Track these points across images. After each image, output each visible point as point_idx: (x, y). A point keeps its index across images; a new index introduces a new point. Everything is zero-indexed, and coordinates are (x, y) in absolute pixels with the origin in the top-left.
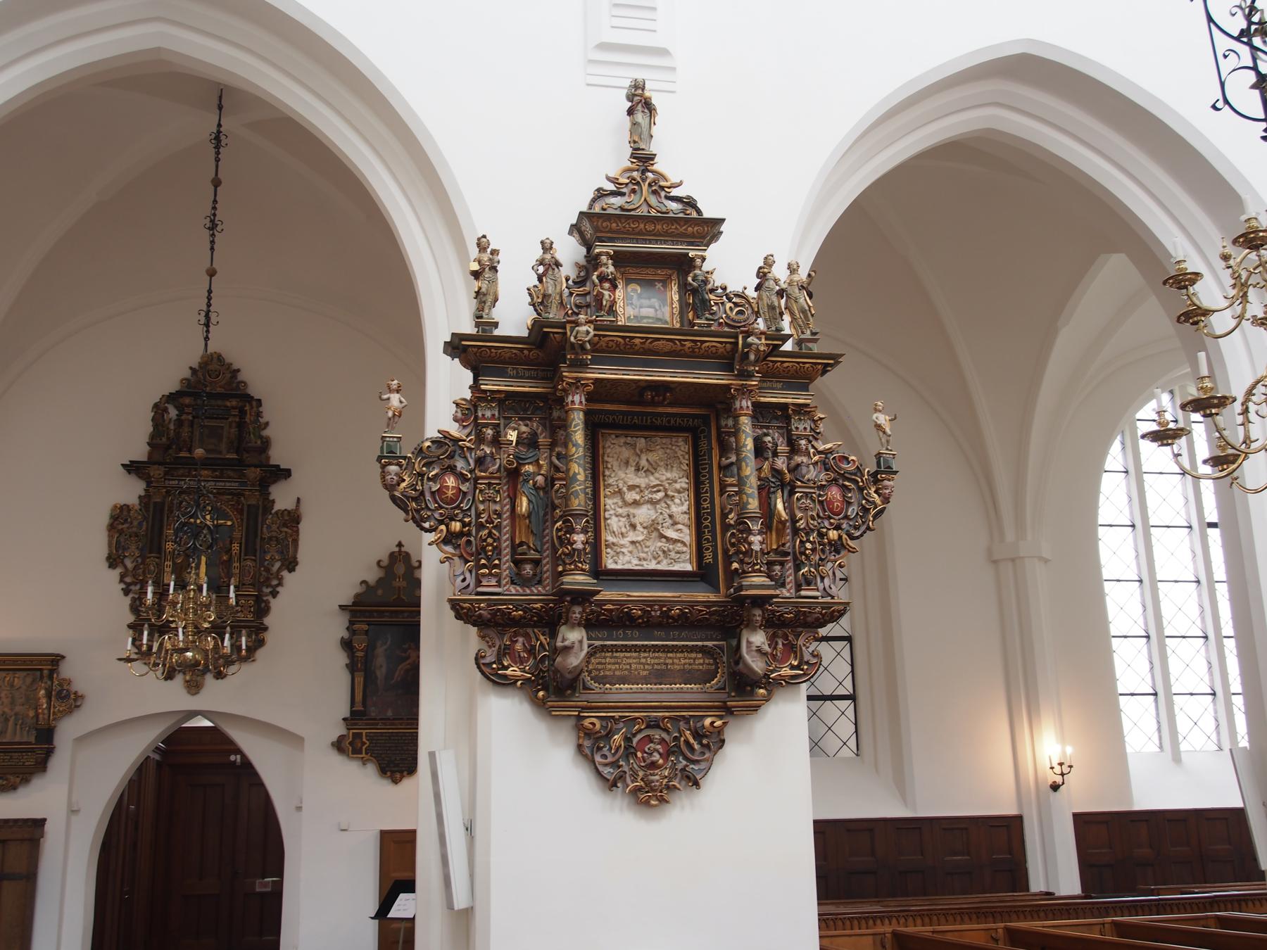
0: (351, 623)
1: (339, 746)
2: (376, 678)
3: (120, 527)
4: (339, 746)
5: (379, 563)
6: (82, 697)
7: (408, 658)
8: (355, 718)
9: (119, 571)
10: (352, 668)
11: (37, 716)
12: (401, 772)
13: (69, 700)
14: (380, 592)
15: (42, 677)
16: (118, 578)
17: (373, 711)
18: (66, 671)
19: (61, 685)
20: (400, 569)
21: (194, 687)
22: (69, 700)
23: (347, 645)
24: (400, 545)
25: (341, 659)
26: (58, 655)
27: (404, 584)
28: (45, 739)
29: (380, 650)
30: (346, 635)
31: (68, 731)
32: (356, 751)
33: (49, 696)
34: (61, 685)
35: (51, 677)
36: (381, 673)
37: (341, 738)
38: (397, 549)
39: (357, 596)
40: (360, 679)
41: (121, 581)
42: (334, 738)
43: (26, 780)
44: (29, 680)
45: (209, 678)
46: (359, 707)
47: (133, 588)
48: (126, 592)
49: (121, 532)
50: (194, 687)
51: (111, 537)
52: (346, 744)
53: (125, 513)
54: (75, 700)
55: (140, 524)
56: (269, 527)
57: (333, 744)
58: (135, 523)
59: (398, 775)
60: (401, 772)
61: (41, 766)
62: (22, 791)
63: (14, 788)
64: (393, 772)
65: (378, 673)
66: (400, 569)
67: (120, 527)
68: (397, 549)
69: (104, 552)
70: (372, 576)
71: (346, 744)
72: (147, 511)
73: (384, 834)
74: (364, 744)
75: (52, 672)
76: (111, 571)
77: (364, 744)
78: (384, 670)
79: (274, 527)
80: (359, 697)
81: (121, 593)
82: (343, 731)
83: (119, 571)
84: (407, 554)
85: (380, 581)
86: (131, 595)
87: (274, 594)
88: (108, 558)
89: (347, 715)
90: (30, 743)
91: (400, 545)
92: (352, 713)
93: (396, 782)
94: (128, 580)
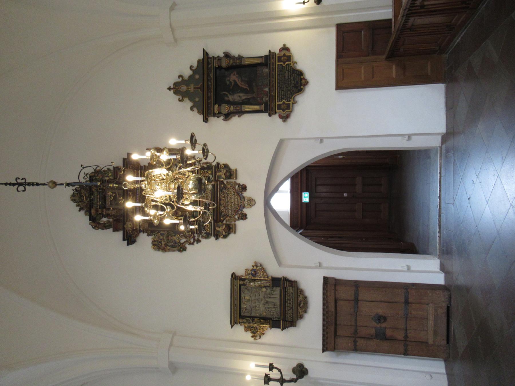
0: (214, 115)
1: (285, 118)
2: (246, 99)
3: (163, 245)
4: (285, 118)
5: (180, 101)
6: (255, 263)
8: (269, 110)
9: (187, 246)
10: (241, 113)
11: (265, 287)
12: (301, 79)
13: (257, 270)
14: (197, 99)
15: (244, 285)
16: (191, 246)
17: (265, 99)
18: (241, 272)
19: (248, 274)
20: (184, 88)
21: (251, 202)
23: (227, 117)
24: (169, 89)
25: (235, 120)
26: (232, 277)
27: (192, 86)
28: (276, 282)
29: (231, 98)
30: (222, 118)
31: (274, 270)
33: (254, 281)
34: (248, 274)
35: (244, 280)
36: (243, 96)
37: (281, 117)
38: (172, 90)
39: (199, 112)
40: (247, 108)
41: (193, 244)
42: (280, 121)
43: (301, 292)
44: (246, 292)
45: (245, 194)
46: (262, 107)
47: (196, 238)
48: (199, 241)
49: (166, 245)
51: (169, 250)
52: (284, 114)
53: (156, 243)
54: (257, 266)
55: (162, 235)
57: (284, 121)
58: (161, 237)
59: (303, 81)
60: (301, 79)
61: (293, 284)
62: (308, 293)
63: (305, 298)
64: (301, 85)
65: (244, 98)
66: (184, 88)
67: (163, 245)
68: (172, 90)
69: (177, 254)
70: (188, 104)
71: (284, 114)
72: (155, 231)
73: (339, 87)
74: (284, 103)
75: (241, 279)
76: (187, 250)
77: (284, 103)
78: (241, 95)
80: (256, 108)
81: (199, 244)
82: (277, 115)
83: (187, 246)
84: (175, 84)
85: (190, 100)
86: (200, 239)
88: (180, 251)
89: (267, 114)
91: (169, 89)
92: (265, 111)
93: (307, 83)
94: (192, 240)
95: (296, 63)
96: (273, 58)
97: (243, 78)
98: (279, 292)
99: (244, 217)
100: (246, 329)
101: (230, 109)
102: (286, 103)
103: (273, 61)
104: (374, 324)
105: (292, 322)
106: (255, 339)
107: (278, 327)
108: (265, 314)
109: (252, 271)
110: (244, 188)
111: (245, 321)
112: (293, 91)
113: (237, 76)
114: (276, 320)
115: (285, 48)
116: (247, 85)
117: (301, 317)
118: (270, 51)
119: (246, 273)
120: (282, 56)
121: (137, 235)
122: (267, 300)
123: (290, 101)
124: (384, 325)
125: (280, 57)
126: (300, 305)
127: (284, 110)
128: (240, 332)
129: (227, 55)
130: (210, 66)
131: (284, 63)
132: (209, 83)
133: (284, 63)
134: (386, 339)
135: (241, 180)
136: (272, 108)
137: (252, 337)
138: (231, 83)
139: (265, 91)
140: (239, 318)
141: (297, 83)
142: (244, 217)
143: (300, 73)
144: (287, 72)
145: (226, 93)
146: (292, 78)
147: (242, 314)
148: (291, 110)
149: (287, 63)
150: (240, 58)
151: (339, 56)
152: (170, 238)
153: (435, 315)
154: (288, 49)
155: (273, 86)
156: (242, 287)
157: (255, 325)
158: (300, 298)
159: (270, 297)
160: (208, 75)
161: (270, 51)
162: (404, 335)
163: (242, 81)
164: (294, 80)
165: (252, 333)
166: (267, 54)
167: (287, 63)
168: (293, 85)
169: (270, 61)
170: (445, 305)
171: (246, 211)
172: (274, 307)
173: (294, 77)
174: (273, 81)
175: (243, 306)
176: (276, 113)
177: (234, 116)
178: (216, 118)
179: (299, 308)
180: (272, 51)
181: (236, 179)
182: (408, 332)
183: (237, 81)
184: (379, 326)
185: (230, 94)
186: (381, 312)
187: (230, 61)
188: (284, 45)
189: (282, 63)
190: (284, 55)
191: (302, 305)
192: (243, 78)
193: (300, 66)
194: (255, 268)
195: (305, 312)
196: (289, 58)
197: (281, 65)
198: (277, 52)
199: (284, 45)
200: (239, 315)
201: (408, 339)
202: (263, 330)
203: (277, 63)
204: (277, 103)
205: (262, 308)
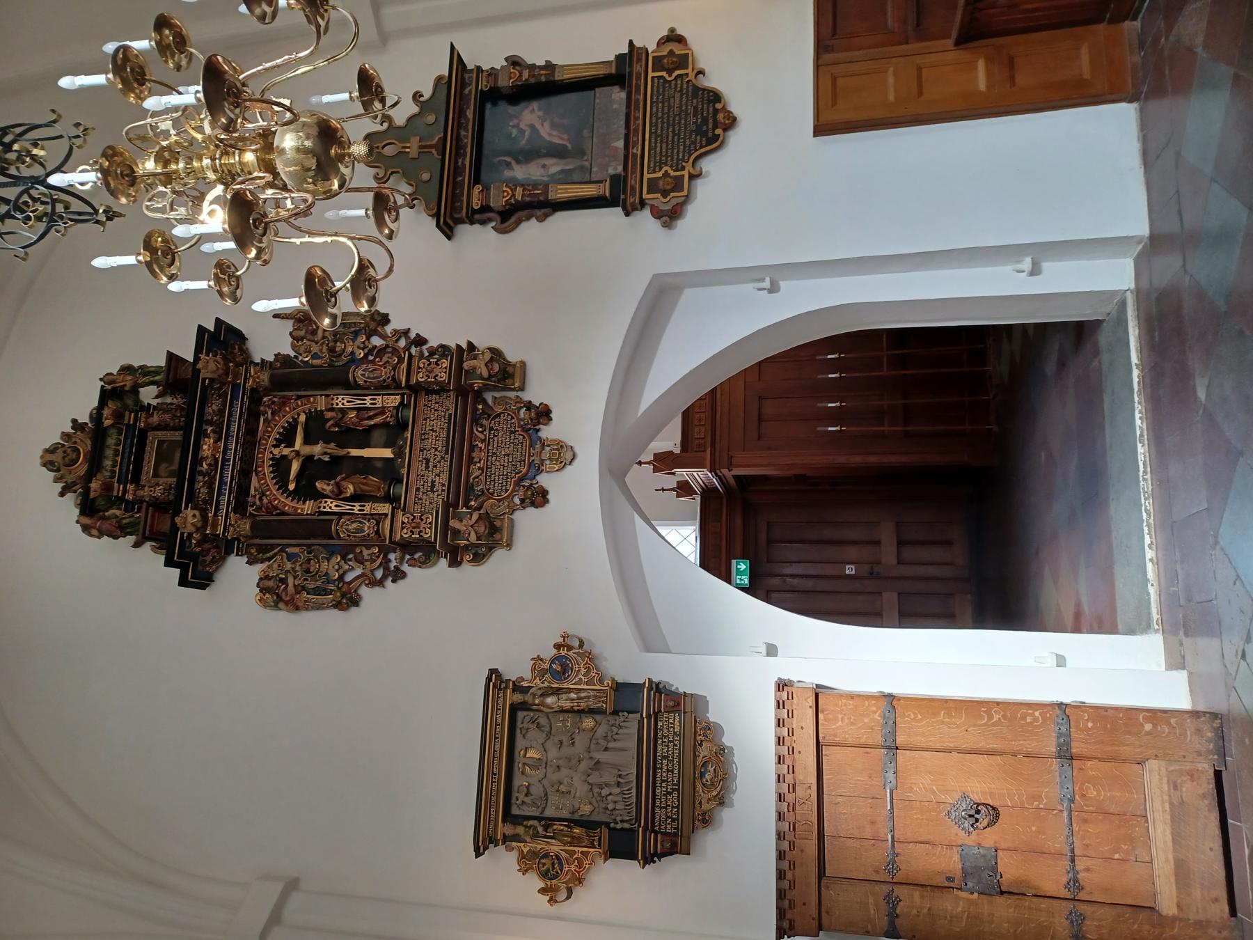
2: (562, 171)
3: (291, 588)
4: (670, 217)
7: (532, 127)
9: (364, 591)
12: (716, 111)
13: (568, 658)
15: (524, 706)
16: (377, 590)
18: (517, 668)
21: (563, 455)
22: (568, 658)
26: (489, 679)
28: (625, 693)
31: (626, 662)
32: (678, 185)
33: (557, 692)
37: (657, 214)
41: (380, 583)
44: (535, 736)
45: (547, 432)
47: (392, 565)
48: (399, 575)
49: (300, 589)
50: (563, 455)
51: (308, 606)
53: (271, 583)
54: (570, 648)
55: (290, 557)
56: (315, 356)
57: (667, 225)
58: (289, 566)
59: (721, 116)
60: (716, 111)
63: (722, 753)
67: (291, 588)
69: (332, 616)
72: (273, 547)
73: (822, 129)
74: (666, 174)
75: (517, 688)
76: (363, 604)
77: (666, 174)
79: (315, 349)
81: (401, 583)
82: (647, 212)
83: (364, 591)
86: (405, 568)
87: (420, 341)
89: (618, 210)
90: (641, 722)
93: (731, 122)
94: (379, 574)
95: (701, 72)
96: (639, 60)
97: (556, 120)
98: (634, 730)
99: (539, 498)
100: (527, 862)
101: (513, 195)
102: (673, 174)
103: (638, 68)
104: (958, 834)
105: (676, 835)
106: (552, 900)
107: (629, 855)
108: (586, 809)
109: (552, 661)
110: (544, 414)
111: (520, 830)
112: (694, 143)
113: (540, 113)
114: (622, 829)
115: (674, 38)
116: (565, 136)
117: (706, 820)
118: (631, 43)
119: (534, 668)
120: (664, 57)
121: (220, 561)
122: (598, 756)
123: (683, 168)
124: (990, 837)
125: (658, 61)
126: (702, 775)
127: (665, 193)
128: (505, 878)
129: (514, 62)
130: (466, 92)
131: (670, 72)
132: (463, 133)
133: (670, 72)
134: (1002, 893)
135: (535, 394)
136: (633, 189)
137: (542, 891)
138: (522, 132)
139: (616, 148)
140: (504, 821)
141: (705, 121)
142: (539, 498)
143: (715, 97)
144: (678, 95)
145: (508, 159)
146: (691, 110)
147: (515, 811)
148: (685, 193)
149: (677, 72)
150: (549, 66)
151: (822, 47)
152: (314, 567)
153: (1171, 804)
154: (680, 40)
155: (636, 130)
156: (521, 714)
157: (555, 848)
158: (704, 752)
159: (606, 749)
160: (460, 113)
161: (631, 43)
162: (1065, 880)
163: (553, 126)
164: (695, 115)
165: (544, 875)
166: (625, 50)
167: (677, 72)
168: (693, 127)
169: (631, 66)
170: (1206, 769)
171: (544, 480)
172: (618, 784)
173: (696, 108)
174: (637, 119)
175: (519, 781)
176: (643, 204)
177: (528, 219)
178: (477, 226)
179: (699, 787)
180: (638, 44)
181: (522, 389)
182: (1080, 865)
183: (538, 126)
184: (971, 840)
185: (518, 162)
186: (978, 790)
187: (521, 73)
188: (672, 30)
189: (664, 74)
190: (671, 53)
191: (708, 777)
192: (556, 120)
193: (713, 81)
194: (563, 652)
195: (721, 801)
196: (683, 61)
197: (662, 77)
198: (652, 47)
199: (672, 30)
200: (503, 816)
201: (1082, 896)
202: (580, 865)
203: (651, 74)
204: (646, 176)
205: (581, 789)
